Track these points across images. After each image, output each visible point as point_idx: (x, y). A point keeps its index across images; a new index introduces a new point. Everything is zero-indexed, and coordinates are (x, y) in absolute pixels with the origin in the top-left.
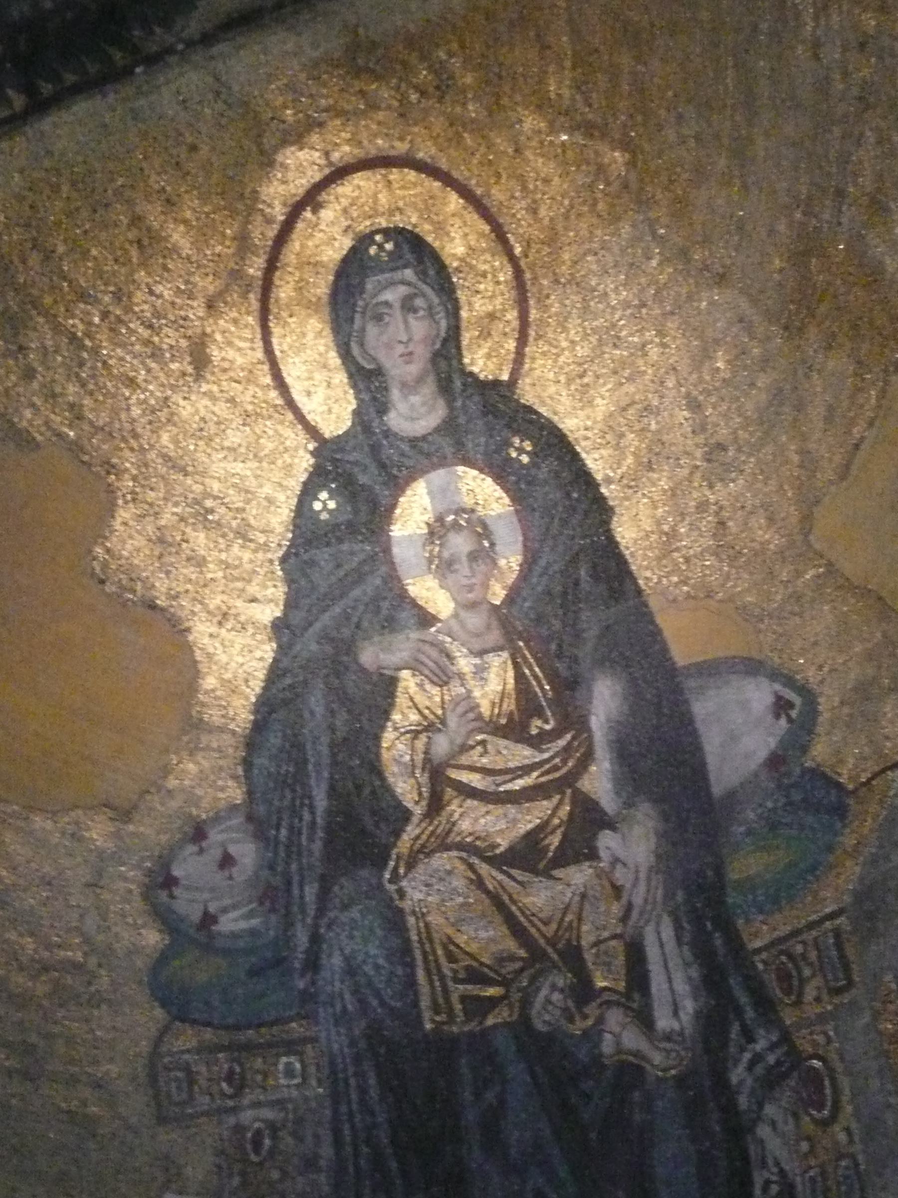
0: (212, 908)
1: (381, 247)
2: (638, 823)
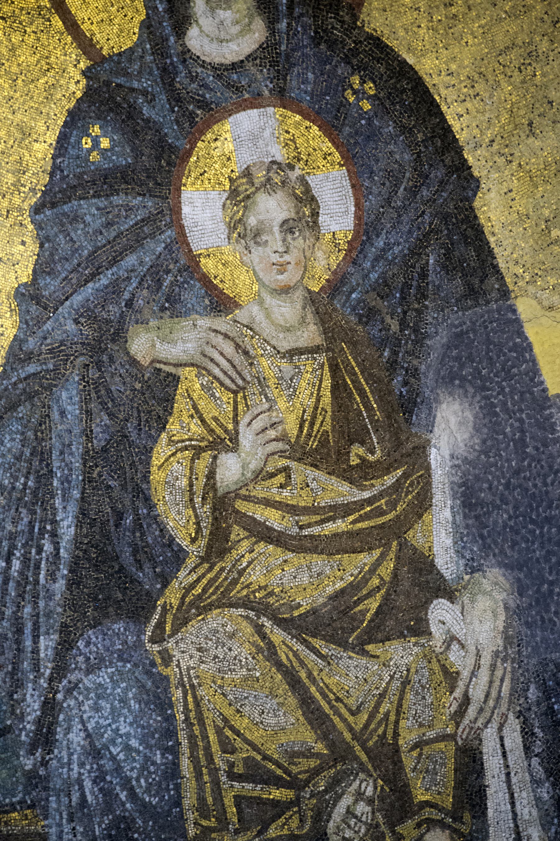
2: (485, 593)
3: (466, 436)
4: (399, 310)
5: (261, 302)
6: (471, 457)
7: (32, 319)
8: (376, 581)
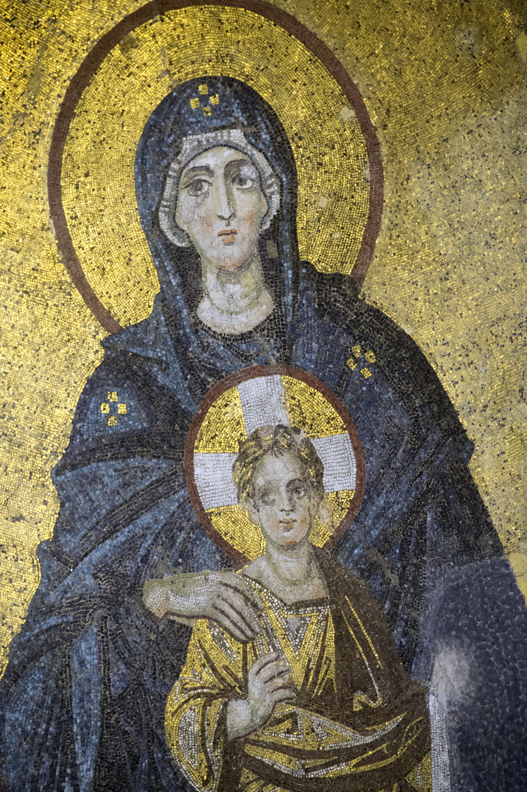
1: (204, 99)
3: (463, 684)
4: (399, 565)
5: (269, 558)
6: (467, 704)
7: (53, 574)
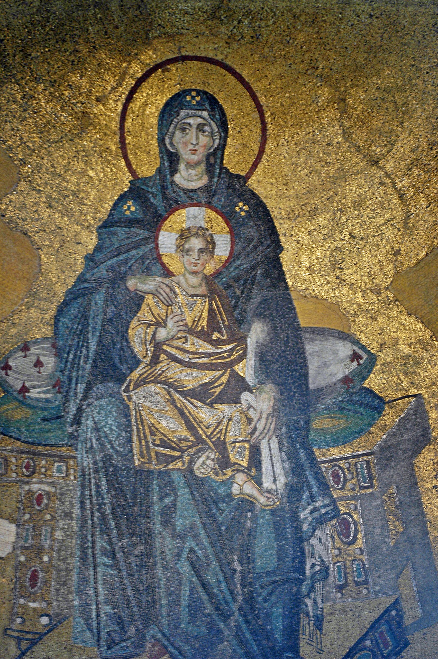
0: (27, 384)
8: (219, 382)
